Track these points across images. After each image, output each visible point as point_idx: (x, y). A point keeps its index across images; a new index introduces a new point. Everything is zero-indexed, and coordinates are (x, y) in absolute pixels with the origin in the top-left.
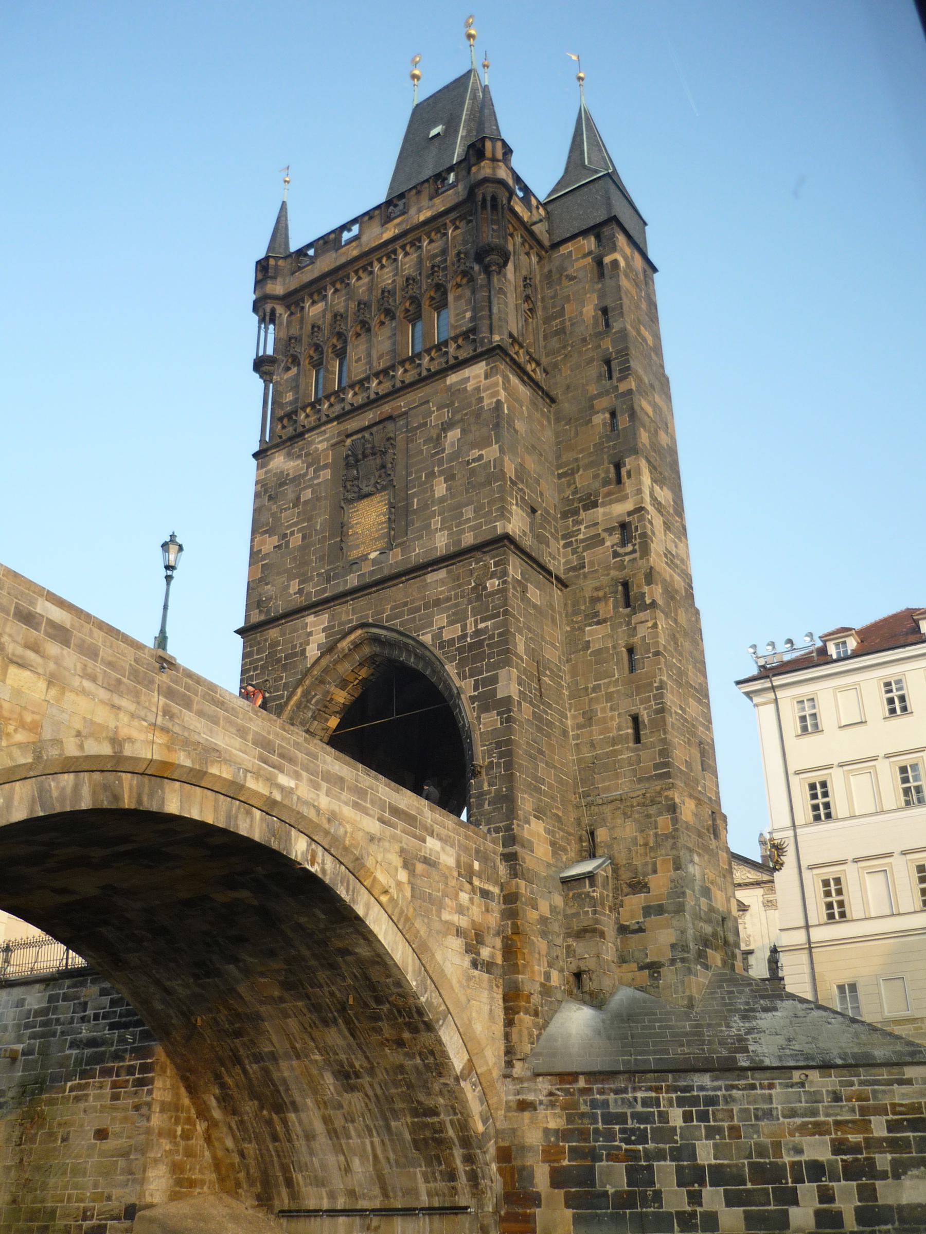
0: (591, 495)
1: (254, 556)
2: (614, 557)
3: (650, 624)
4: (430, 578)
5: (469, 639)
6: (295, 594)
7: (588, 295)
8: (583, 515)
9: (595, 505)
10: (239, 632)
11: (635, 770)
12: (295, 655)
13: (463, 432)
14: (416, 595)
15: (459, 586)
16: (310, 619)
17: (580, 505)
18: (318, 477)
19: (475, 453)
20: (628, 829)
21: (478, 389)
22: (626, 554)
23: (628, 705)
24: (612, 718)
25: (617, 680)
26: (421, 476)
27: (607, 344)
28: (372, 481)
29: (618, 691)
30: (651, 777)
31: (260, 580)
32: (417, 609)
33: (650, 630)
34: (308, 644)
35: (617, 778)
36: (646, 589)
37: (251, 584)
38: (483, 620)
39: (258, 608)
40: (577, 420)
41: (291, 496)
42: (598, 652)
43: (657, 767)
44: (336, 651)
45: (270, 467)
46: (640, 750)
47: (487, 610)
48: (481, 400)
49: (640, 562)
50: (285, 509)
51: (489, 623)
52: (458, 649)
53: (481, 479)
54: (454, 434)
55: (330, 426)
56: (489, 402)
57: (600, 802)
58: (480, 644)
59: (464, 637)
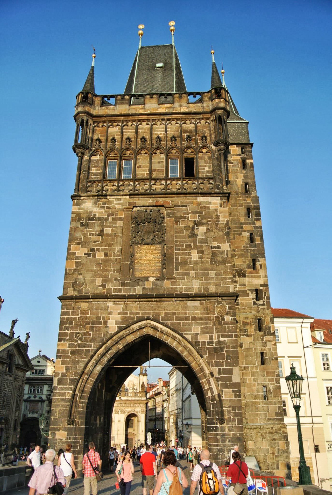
0: (242, 270)
1: (70, 255)
2: (254, 305)
3: (273, 343)
4: (190, 303)
5: (214, 345)
6: (99, 286)
7: (239, 174)
8: (238, 279)
9: (244, 276)
10: (60, 298)
11: (266, 414)
12: (100, 323)
13: (208, 229)
14: (181, 310)
15: (208, 313)
16: (110, 304)
17: (236, 273)
18: (116, 223)
20: (264, 444)
21: (216, 210)
22: (260, 305)
23: (261, 380)
24: (254, 385)
25: (257, 366)
26: (183, 245)
27: (249, 200)
28: (151, 238)
29: (257, 372)
30: (274, 419)
31: (75, 271)
32: (182, 319)
33: (273, 346)
34: (109, 319)
35: (257, 416)
36: (271, 325)
37: (68, 271)
38: (223, 336)
39: (73, 286)
40: (234, 231)
42: (247, 350)
43: (277, 414)
44: (129, 328)
45: (83, 206)
46: (269, 405)
47: (225, 332)
48: (218, 217)
50: (93, 235)
52: (207, 348)
54: (202, 230)
55: (124, 197)
56: (223, 219)
57: (250, 427)
58: (222, 349)
59: (211, 343)
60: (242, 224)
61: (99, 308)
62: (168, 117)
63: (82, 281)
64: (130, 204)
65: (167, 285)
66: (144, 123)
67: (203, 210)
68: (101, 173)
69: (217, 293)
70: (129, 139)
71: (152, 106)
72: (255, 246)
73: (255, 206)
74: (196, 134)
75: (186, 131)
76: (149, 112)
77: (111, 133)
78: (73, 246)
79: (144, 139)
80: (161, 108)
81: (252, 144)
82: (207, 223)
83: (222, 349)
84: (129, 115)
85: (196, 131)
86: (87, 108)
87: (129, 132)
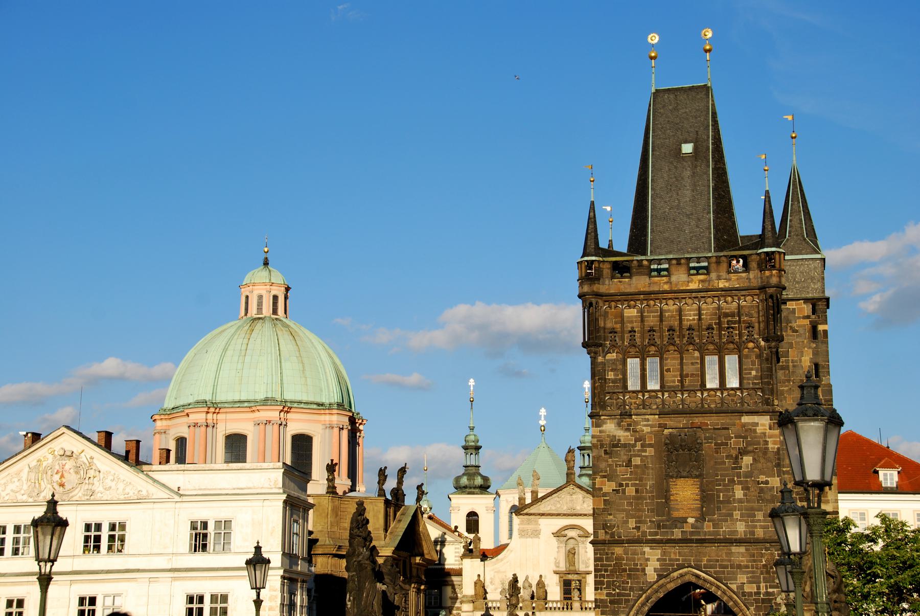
4: (734, 549)
12: (638, 570)
13: (754, 459)
15: (754, 561)
16: (647, 549)
18: (646, 451)
19: (763, 478)
28: (687, 469)
32: (726, 567)
48: (766, 443)
51: (775, 590)
53: (768, 497)
54: (747, 460)
59: (758, 593)
61: (635, 553)
62: (702, 294)
64: (660, 426)
65: (708, 527)
66: (671, 302)
67: (748, 434)
68: (620, 379)
69: (764, 539)
70: (651, 330)
73: (826, 401)
74: (740, 318)
75: (726, 315)
77: (628, 317)
78: (598, 480)
79: (671, 329)
80: (692, 281)
82: (753, 452)
83: (770, 601)
84: (650, 293)
87: (652, 320)
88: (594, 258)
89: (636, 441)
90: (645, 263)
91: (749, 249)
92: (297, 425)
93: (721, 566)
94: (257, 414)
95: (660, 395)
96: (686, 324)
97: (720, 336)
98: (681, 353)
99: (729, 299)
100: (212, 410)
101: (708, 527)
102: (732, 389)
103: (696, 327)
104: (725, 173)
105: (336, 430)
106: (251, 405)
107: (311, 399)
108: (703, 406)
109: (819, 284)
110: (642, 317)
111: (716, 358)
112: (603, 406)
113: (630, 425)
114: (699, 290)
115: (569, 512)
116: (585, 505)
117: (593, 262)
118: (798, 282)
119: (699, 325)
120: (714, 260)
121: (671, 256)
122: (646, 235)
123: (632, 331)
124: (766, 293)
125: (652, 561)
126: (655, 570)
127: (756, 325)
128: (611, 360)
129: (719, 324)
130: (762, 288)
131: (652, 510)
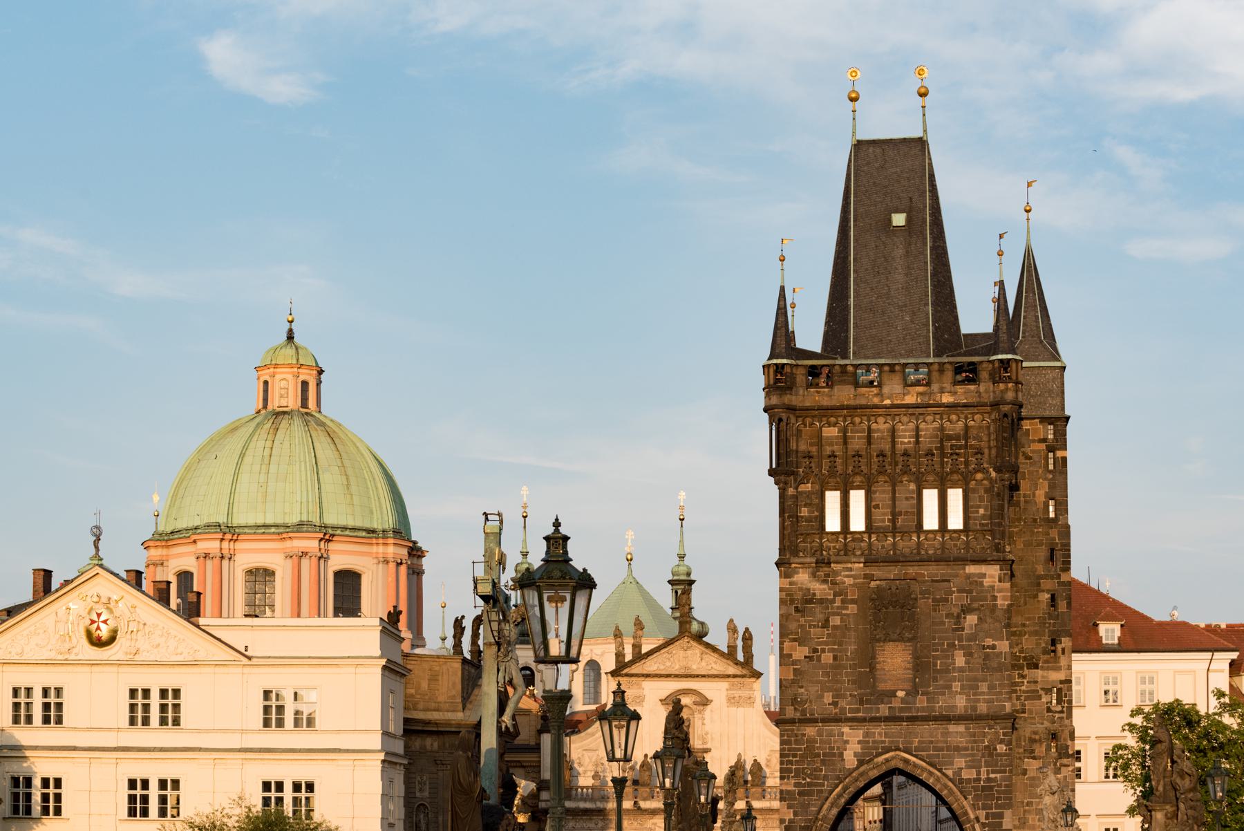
4: (952, 728)
8: (1026, 671)
9: (1036, 667)
12: (834, 755)
13: (980, 619)
15: (975, 742)
16: (846, 730)
18: (847, 608)
19: (989, 642)
21: (993, 587)
27: (1054, 533)
31: (793, 681)
41: (821, 616)
48: (995, 598)
49: (1067, 722)
54: (972, 619)
60: (1040, 577)
62: (921, 411)
63: (805, 697)
64: (866, 576)
65: (921, 702)
66: (881, 420)
71: (894, 393)
72: (1057, 617)
73: (1062, 545)
75: (950, 438)
76: (888, 402)
77: (828, 438)
79: (882, 454)
80: (909, 393)
81: (1068, 418)
84: (855, 408)
85: (966, 438)
86: (789, 399)
87: (857, 443)
88: (785, 361)
89: (835, 596)
90: (850, 369)
91: (979, 355)
92: (342, 557)
93: (935, 749)
94: (288, 544)
95: (866, 538)
96: (900, 448)
97: (942, 463)
98: (894, 486)
99: (954, 417)
100: (228, 536)
101: (921, 701)
102: (955, 531)
103: (912, 453)
104: (946, 253)
105: (392, 565)
106: (282, 531)
107: (359, 524)
108: (919, 553)
109: (1058, 400)
110: (845, 438)
111: (935, 492)
112: (795, 553)
113: (828, 575)
114: (907, 402)
115: (682, 672)
116: (704, 663)
117: (784, 365)
118: (1032, 396)
119: (917, 450)
120: (936, 367)
121: (882, 361)
122: (847, 331)
123: (833, 455)
124: (999, 411)
125: (852, 743)
126: (855, 754)
127: (986, 451)
128: (805, 492)
129: (942, 448)
130: (995, 405)
131: (854, 682)
